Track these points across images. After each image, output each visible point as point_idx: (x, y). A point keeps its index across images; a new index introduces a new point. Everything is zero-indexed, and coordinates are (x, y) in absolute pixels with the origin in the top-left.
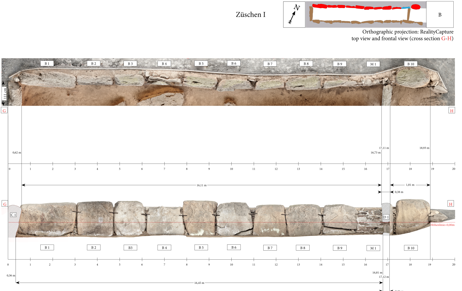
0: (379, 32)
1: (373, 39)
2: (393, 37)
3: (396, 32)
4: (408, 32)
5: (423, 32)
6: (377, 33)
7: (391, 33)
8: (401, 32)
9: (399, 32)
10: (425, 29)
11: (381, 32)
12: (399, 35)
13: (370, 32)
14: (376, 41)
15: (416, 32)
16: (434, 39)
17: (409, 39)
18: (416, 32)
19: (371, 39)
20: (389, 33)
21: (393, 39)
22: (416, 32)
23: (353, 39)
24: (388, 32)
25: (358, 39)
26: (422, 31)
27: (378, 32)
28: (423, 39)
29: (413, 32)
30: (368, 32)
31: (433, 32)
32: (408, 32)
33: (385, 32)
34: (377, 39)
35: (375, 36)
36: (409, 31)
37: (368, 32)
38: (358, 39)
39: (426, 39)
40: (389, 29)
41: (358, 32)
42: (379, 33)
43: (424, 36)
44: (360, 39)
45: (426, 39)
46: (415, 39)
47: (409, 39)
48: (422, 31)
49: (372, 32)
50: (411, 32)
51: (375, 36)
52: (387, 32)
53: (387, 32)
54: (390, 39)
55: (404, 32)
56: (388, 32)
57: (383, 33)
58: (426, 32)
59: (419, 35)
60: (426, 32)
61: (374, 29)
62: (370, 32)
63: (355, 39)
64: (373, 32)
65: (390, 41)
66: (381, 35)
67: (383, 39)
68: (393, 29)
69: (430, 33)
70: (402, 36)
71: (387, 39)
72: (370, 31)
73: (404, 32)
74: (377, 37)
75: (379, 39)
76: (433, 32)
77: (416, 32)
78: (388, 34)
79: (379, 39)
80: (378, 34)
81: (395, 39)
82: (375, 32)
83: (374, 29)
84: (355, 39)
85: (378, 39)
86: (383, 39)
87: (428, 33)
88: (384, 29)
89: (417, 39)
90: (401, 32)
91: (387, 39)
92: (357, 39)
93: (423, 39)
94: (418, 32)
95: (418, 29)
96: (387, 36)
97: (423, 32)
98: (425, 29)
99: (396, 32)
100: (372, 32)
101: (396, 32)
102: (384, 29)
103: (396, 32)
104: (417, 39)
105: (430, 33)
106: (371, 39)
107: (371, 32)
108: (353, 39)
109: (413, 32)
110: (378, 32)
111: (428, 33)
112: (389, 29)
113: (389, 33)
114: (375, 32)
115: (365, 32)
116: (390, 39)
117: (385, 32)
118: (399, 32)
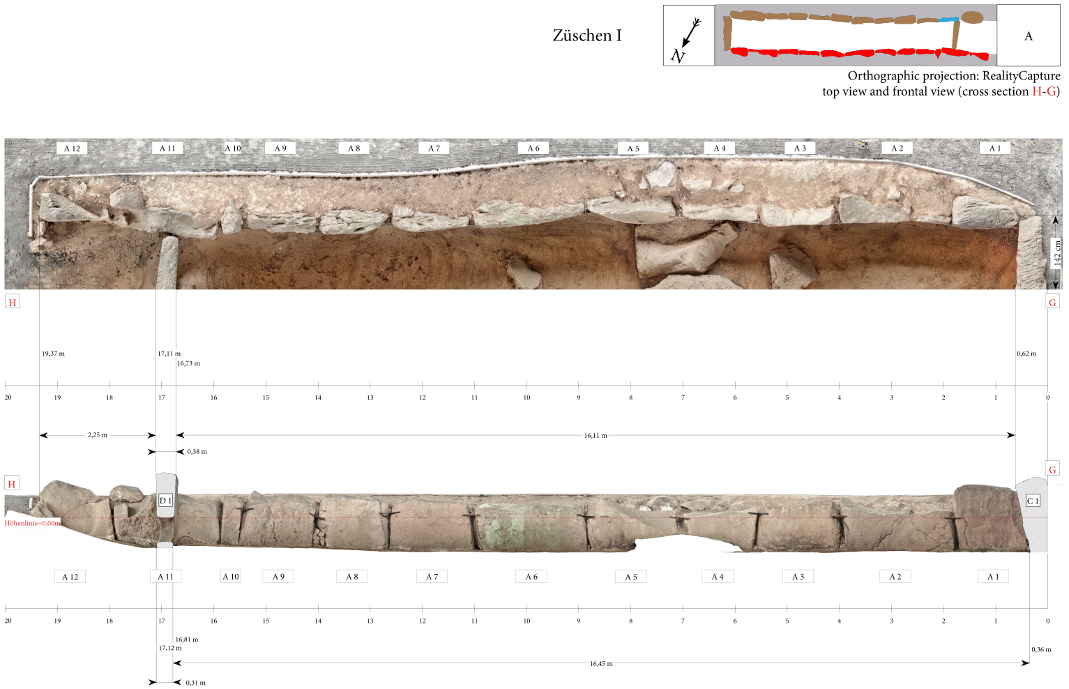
0: (887, 76)
1: (873, 93)
2: (919, 89)
3: (927, 77)
4: (953, 77)
5: (989, 76)
6: (883, 78)
7: (914, 78)
8: (937, 77)
9: (933, 77)
10: (993, 70)
11: (890, 77)
12: (933, 84)
13: (866, 77)
14: (879, 96)
15: (973, 76)
17: (956, 93)
18: (972, 77)
19: (868, 93)
20: (911, 78)
21: (918, 93)
22: (973, 76)
23: (826, 93)
24: (907, 76)
25: (836, 92)
26: (986, 74)
27: (883, 76)
28: (990, 92)
29: (966, 77)
30: (862, 77)
32: (953, 77)
33: (900, 76)
34: (882, 93)
35: (876, 85)
36: (957, 74)
37: (862, 77)
38: (836, 92)
39: (996, 93)
40: (909, 70)
41: (836, 75)
42: (886, 78)
43: (991, 85)
44: (842, 92)
45: (996, 93)
46: (972, 92)
47: (956, 93)
48: (986, 74)
49: (870, 76)
50: (962, 77)
51: (876, 85)
52: (905, 75)
53: (905, 75)
54: (911, 92)
55: (943, 77)
56: (907, 76)
57: (897, 78)
58: (996, 77)
59: (980, 84)
60: (996, 77)
61: (874, 70)
62: (866, 77)
63: (829, 93)
64: (874, 77)
65: (911, 96)
66: (891, 84)
67: (896, 92)
68: (920, 70)
69: (1005, 78)
70: (940, 85)
71: (904, 93)
72: (866, 73)
73: (943, 77)
74: (883, 87)
75: (886, 93)
77: (972, 77)
78: (907, 80)
79: (886, 93)
80: (883, 81)
81: (923, 93)
82: (877, 77)
83: (874, 70)
84: (829, 93)
85: (885, 93)
86: (896, 92)
87: (1002, 78)
88: (899, 70)
89: (976, 92)
90: (937, 77)
91: (904, 93)
92: (835, 93)
93: (990, 92)
94: (977, 77)
95: (979, 70)
96: (905, 85)
97: (989, 76)
98: (993, 70)
99: (926, 76)
100: (870, 76)
101: (926, 76)
102: (899, 70)
103: (927, 77)
104: (976, 92)
105: (1005, 78)
106: (868, 93)
107: (868, 76)
108: (826, 93)
109: (966, 77)
110: (883, 76)
111: (1002, 78)
112: (909, 70)
113: (911, 78)
114: (877, 77)
115: (853, 75)
116: (911, 92)
117: (900, 76)
118: (933, 77)
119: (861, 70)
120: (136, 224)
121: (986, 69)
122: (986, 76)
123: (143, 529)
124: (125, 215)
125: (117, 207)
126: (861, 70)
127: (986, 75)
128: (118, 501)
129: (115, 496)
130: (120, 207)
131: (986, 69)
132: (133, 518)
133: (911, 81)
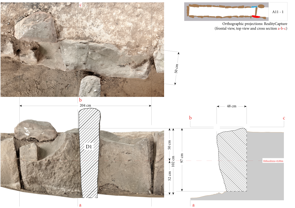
3: (246, 24)
5: (266, 24)
6: (233, 24)
7: (242, 24)
8: (249, 24)
10: (267, 22)
16: (273, 29)
28: (265, 29)
30: (227, 24)
31: (273, 24)
35: (231, 26)
37: (227, 24)
40: (241, 22)
41: (219, 24)
42: (234, 24)
50: (257, 24)
51: (231, 26)
52: (239, 24)
53: (239, 24)
55: (251, 24)
57: (237, 24)
59: (263, 26)
61: (230, 22)
64: (230, 24)
73: (251, 24)
74: (233, 27)
76: (273, 24)
82: (231, 24)
83: (230, 22)
88: (238, 22)
89: (261, 29)
90: (249, 24)
93: (265, 29)
95: (263, 22)
96: (239, 26)
97: (266, 24)
98: (267, 22)
99: (246, 24)
101: (246, 24)
102: (238, 22)
103: (246, 24)
104: (261, 29)
107: (228, 24)
112: (241, 22)
114: (231, 24)
115: (224, 24)
119: (226, 22)
120: (48, 61)
121: (265, 22)
122: (265, 24)
123: (57, 175)
124: (34, 49)
125: (24, 39)
126: (226, 22)
127: (265, 24)
128: (24, 140)
129: (20, 134)
130: (27, 40)
131: (265, 22)
132: (44, 161)
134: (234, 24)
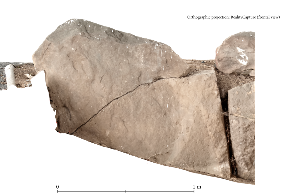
4: (221, 17)
5: (233, 17)
8: (216, 17)
9: (215, 17)
11: (201, 17)
29: (225, 17)
30: (192, 17)
32: (221, 17)
33: (204, 17)
37: (192, 17)
42: (200, 18)
78: (206, 19)
82: (197, 17)
90: (216, 17)
97: (233, 17)
99: (213, 17)
101: (213, 17)
109: (225, 17)
114: (197, 17)
117: (204, 17)
118: (215, 17)
133: (208, 19)
134: (200, 18)
